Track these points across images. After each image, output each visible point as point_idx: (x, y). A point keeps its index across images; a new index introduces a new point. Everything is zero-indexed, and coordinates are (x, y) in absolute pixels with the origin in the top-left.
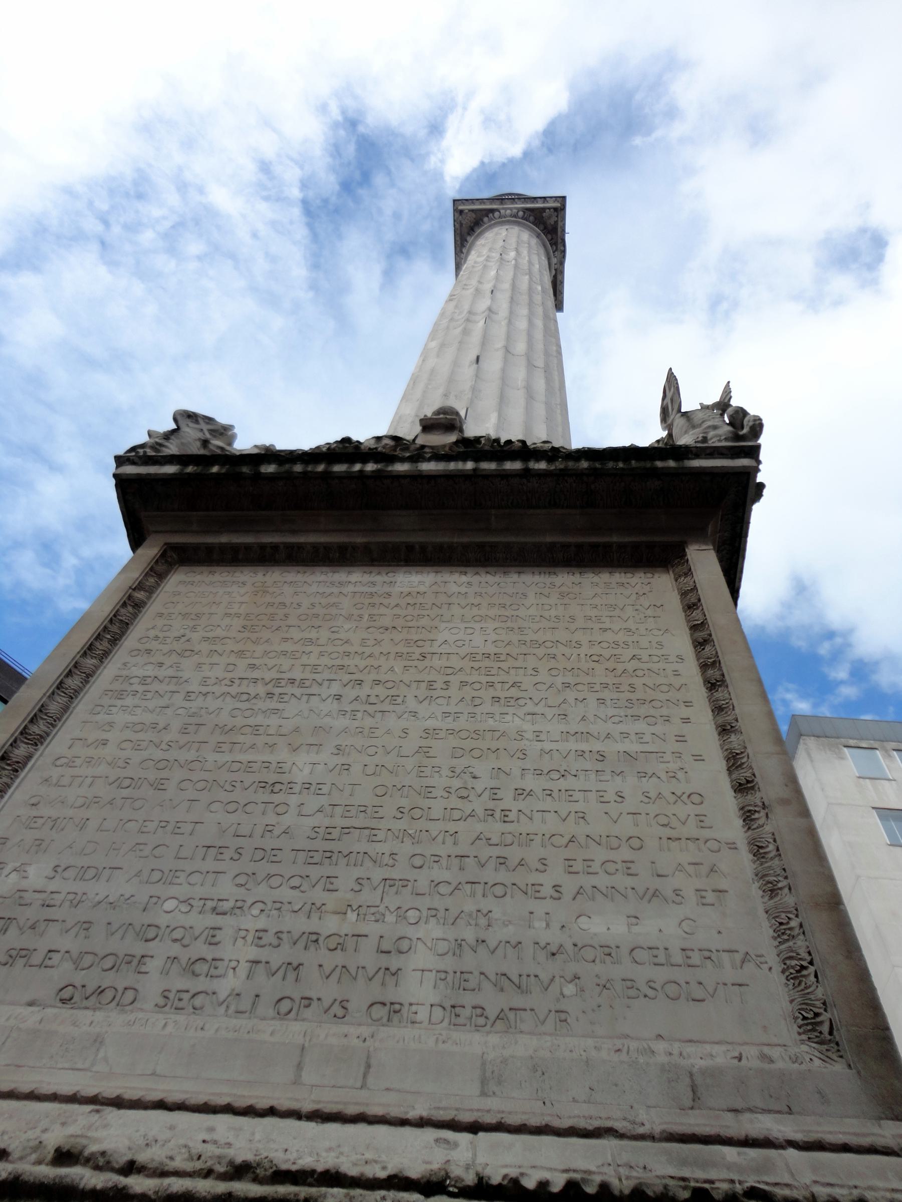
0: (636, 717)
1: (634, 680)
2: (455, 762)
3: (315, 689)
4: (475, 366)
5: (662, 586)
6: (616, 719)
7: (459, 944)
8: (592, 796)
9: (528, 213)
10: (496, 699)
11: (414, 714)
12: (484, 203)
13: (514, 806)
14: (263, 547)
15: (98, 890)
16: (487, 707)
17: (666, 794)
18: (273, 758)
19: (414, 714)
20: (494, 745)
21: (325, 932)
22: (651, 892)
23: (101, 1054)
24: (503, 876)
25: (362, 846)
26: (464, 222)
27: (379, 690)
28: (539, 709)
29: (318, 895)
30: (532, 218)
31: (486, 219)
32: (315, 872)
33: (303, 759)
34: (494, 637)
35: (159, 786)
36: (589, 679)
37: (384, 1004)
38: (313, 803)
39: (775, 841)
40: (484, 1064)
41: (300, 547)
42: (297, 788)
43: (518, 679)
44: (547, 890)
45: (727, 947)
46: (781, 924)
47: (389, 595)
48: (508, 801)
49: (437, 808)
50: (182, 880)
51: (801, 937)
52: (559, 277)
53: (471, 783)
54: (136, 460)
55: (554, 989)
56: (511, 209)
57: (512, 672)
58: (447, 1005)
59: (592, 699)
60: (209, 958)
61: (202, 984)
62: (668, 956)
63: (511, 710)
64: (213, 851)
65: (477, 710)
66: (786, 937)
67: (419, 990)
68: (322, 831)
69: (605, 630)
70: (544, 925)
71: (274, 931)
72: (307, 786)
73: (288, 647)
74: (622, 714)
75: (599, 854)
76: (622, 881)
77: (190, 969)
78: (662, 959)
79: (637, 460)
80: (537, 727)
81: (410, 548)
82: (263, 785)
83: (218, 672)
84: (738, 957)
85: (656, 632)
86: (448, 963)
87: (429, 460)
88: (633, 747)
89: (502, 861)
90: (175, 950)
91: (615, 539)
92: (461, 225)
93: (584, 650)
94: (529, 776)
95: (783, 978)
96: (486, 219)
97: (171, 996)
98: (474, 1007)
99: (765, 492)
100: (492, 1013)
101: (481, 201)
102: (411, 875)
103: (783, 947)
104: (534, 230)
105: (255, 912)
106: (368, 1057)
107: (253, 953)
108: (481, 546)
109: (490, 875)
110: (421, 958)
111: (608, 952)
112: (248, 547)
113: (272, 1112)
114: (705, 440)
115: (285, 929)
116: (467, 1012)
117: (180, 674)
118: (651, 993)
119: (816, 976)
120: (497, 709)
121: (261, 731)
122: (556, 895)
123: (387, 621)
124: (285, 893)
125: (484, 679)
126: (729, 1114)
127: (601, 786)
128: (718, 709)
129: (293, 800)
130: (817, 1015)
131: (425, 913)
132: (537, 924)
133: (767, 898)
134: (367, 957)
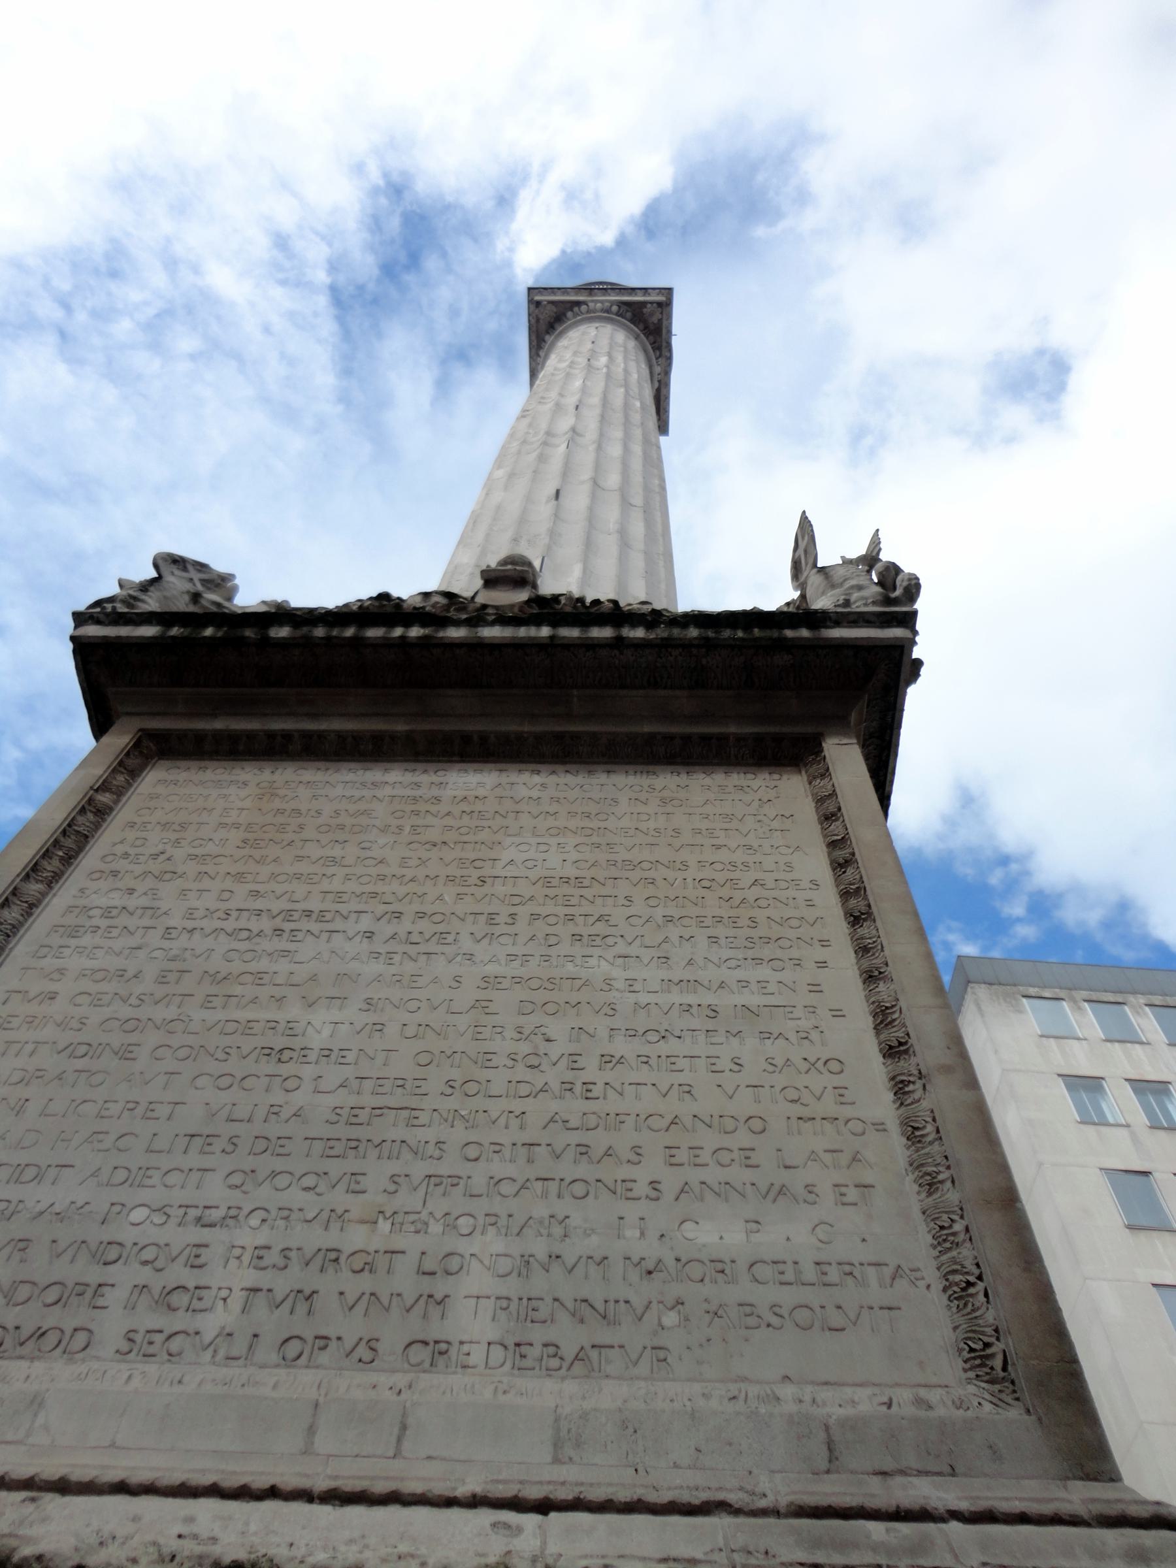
0: (758, 961)
1: (756, 913)
2: (522, 1020)
3: (339, 924)
4: (554, 502)
5: (791, 790)
6: (733, 963)
7: (527, 1261)
8: (701, 1063)
9: (624, 308)
10: (577, 937)
11: (470, 956)
12: (568, 294)
13: (600, 1077)
14: (271, 735)
15: (38, 1196)
16: (565, 948)
17: (797, 1060)
18: (281, 1016)
19: (470, 956)
20: (574, 998)
21: (347, 1249)
22: (776, 1188)
23: (40, 1420)
24: (583, 1170)
26: (541, 317)
27: (424, 925)
28: (633, 950)
29: (339, 1199)
30: (629, 315)
31: (569, 314)
32: (335, 1168)
33: (321, 1017)
34: (574, 856)
35: (126, 1054)
37: (426, 1343)
38: (333, 1075)
39: (934, 1120)
40: (557, 1420)
41: (321, 735)
42: (312, 1056)
43: (606, 911)
44: (641, 1189)
45: (873, 1259)
46: (942, 1228)
47: (438, 800)
49: (499, 1081)
50: (156, 1178)
51: (968, 1244)
52: (663, 391)
53: (543, 1047)
54: (102, 617)
55: (651, 1318)
56: (602, 302)
58: (510, 1342)
60: (191, 1285)
61: (180, 1321)
62: (798, 1272)
63: (596, 952)
64: (198, 1141)
65: (553, 951)
66: (948, 1245)
67: (473, 1323)
68: (345, 1112)
69: (719, 847)
70: (638, 1234)
71: (281, 1247)
72: (326, 1053)
73: (303, 868)
74: (740, 956)
75: (709, 1140)
76: (739, 1175)
77: (165, 1300)
78: (789, 1276)
79: (761, 627)
80: (630, 974)
81: (466, 738)
82: (267, 1052)
84: (888, 1272)
85: (783, 850)
86: (512, 1288)
87: (492, 624)
88: (754, 999)
89: (584, 1150)
90: (145, 1275)
91: (733, 729)
92: (538, 320)
93: (690, 874)
94: (619, 1039)
95: (945, 1298)
96: (569, 314)
97: (138, 1338)
98: (545, 1345)
99: (923, 671)
100: (569, 1351)
101: (564, 290)
102: (463, 1169)
103: (944, 1258)
104: (632, 330)
106: (404, 1415)
107: (251, 1277)
108: (559, 737)
109: (566, 1169)
110: (476, 1280)
111: (721, 1268)
112: (250, 736)
113: (273, 1493)
114: (847, 603)
115: (294, 1245)
116: (536, 1351)
117: (156, 904)
118: (775, 1321)
119: (986, 1295)
120: (578, 950)
122: (654, 1194)
123: (433, 835)
124: (296, 1197)
125: (561, 911)
126: (876, 1480)
127: (713, 1051)
128: (863, 950)
129: (308, 1072)
130: (987, 1345)
131: (481, 1220)
132: (628, 1233)
133: (924, 1195)
134: (404, 1281)
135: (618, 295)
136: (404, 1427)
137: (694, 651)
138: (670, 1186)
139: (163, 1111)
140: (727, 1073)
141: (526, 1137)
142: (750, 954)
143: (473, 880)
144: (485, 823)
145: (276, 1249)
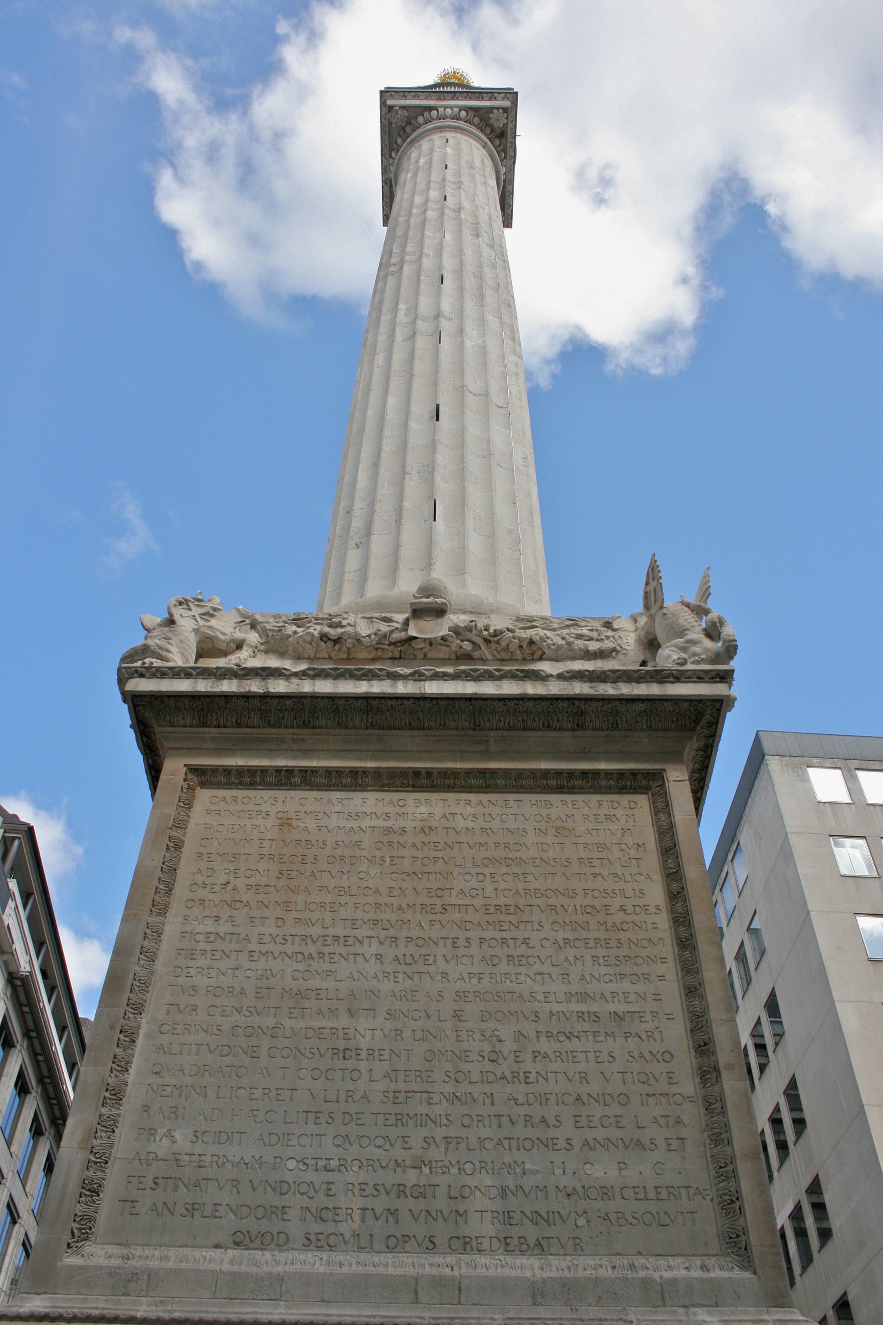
1: (621, 935)
2: (484, 1025)
6: (607, 978)
8: (591, 1056)
9: (471, 113)
11: (444, 975)
14: (278, 770)
16: (503, 967)
17: (646, 1054)
19: (444, 975)
21: (409, 1184)
22: (635, 1141)
24: (529, 1132)
25: (423, 1109)
26: (394, 121)
28: (545, 968)
33: (363, 1024)
36: (585, 934)
37: (459, 1238)
41: (314, 771)
42: (364, 1055)
43: (526, 935)
44: (562, 1143)
45: (684, 1185)
46: (721, 1167)
48: (528, 1064)
50: (294, 1142)
51: (733, 1179)
52: (509, 188)
56: (451, 107)
57: (522, 926)
58: (501, 1236)
59: (588, 954)
60: (331, 1207)
61: (330, 1227)
62: (646, 1193)
63: (523, 970)
65: (496, 970)
66: (723, 1178)
70: (562, 1172)
71: (372, 1184)
72: (371, 1051)
74: (612, 972)
75: (598, 1110)
76: (614, 1133)
78: (641, 1196)
80: (545, 988)
83: (270, 928)
84: (692, 1191)
85: (638, 878)
88: (621, 1008)
91: (603, 766)
92: (390, 124)
94: (543, 1039)
97: (313, 1237)
98: (519, 1238)
100: (532, 1241)
105: (356, 1168)
109: (521, 1132)
110: (479, 1202)
111: (605, 1192)
112: (264, 771)
115: (380, 1183)
117: (236, 930)
118: (634, 1221)
120: (512, 969)
121: (322, 996)
122: (568, 1147)
125: (499, 935)
126: (681, 1310)
130: (738, 1236)
131: (477, 1165)
132: (556, 1172)
133: (712, 1146)
134: (441, 1203)
135: (465, 99)
136: (460, 1290)
137: (577, 703)
138: (577, 1143)
139: (286, 1094)
140: (606, 1063)
141: (494, 1110)
142: (618, 970)
143: (438, 908)
144: (439, 854)
145: (371, 1184)
